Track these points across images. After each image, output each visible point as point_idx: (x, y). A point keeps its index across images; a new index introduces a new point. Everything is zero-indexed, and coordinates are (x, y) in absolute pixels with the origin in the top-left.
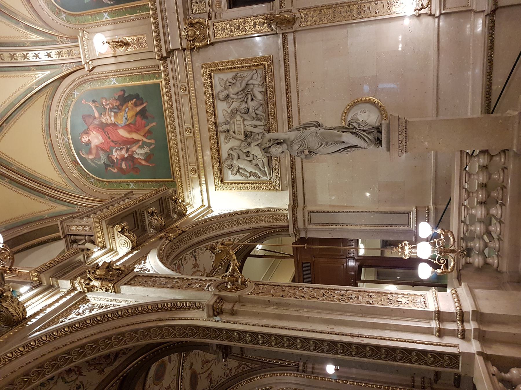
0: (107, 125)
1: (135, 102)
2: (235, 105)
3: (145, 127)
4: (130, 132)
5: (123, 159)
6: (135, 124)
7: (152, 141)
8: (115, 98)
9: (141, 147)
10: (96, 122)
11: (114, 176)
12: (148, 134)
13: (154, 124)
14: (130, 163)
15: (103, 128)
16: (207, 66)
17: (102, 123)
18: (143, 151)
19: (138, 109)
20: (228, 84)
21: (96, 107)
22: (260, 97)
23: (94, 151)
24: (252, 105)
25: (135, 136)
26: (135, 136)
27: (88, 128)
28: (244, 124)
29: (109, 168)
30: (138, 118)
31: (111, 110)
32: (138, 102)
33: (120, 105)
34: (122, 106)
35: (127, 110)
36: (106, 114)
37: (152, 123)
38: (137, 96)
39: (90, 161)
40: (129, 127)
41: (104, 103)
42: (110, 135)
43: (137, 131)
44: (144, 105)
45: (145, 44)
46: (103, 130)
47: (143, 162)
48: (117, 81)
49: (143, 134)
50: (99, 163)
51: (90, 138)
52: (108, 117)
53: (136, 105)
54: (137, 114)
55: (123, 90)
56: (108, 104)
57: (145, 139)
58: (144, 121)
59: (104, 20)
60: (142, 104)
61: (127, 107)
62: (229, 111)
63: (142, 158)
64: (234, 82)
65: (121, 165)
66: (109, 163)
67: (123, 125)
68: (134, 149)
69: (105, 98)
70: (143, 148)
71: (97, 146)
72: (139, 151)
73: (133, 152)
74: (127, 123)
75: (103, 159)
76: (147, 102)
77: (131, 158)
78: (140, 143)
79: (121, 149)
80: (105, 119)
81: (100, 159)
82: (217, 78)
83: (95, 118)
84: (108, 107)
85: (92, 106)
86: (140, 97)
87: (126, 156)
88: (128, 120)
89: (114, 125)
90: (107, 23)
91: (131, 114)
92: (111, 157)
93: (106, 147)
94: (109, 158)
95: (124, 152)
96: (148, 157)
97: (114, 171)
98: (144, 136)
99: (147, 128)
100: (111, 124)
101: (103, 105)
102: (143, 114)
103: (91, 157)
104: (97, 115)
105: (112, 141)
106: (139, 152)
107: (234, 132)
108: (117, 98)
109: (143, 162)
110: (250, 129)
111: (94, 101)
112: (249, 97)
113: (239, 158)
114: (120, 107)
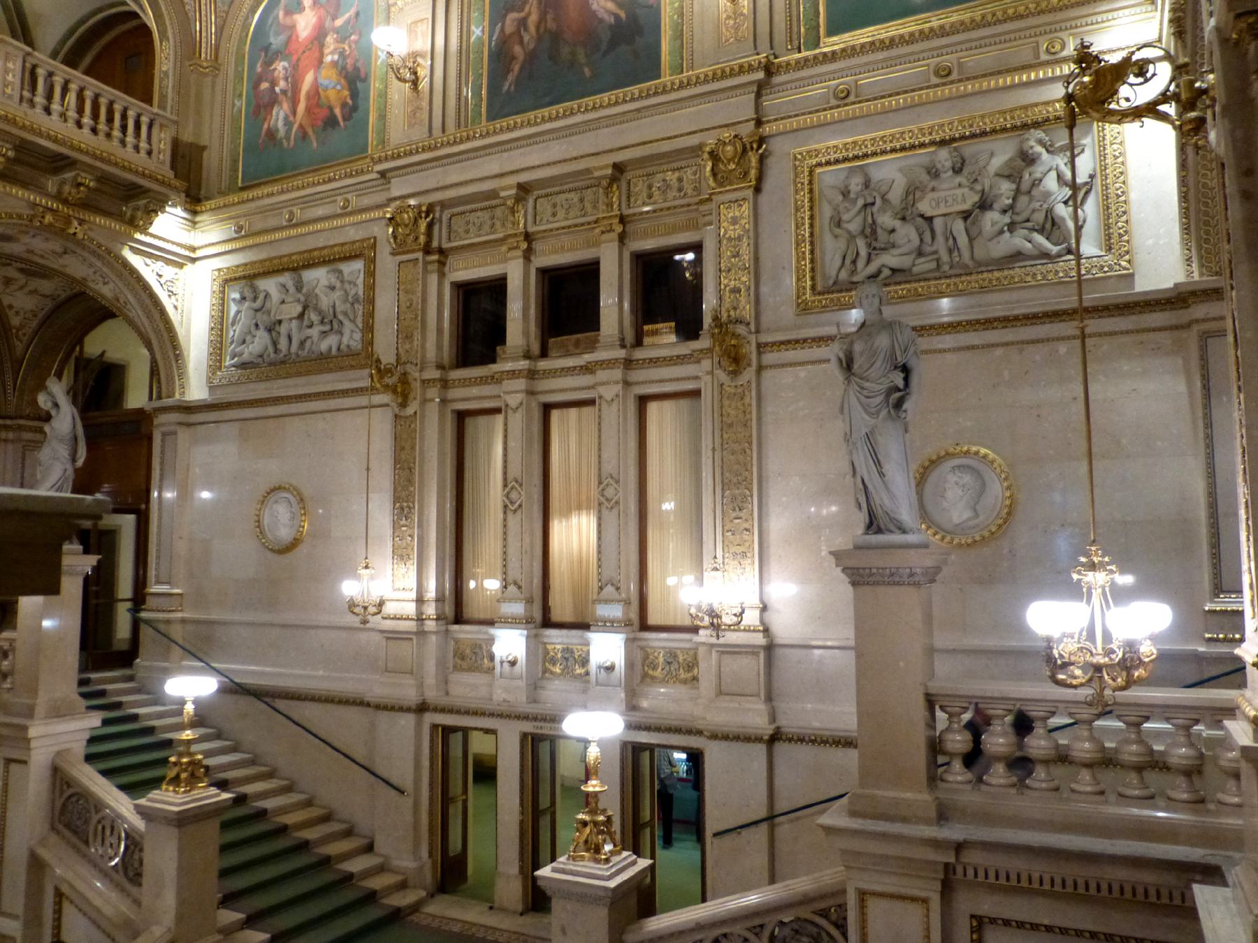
0: (322, 46)
1: (347, 103)
2: (325, 302)
3: (313, 126)
4: (308, 97)
5: (274, 83)
6: (318, 105)
7: (292, 143)
8: (357, 61)
9: (286, 118)
10: (328, 24)
11: (252, 67)
12: (304, 135)
13: (315, 144)
14: (266, 100)
15: (319, 36)
16: (374, 246)
17: (325, 35)
18: (280, 124)
19: (337, 111)
20: (347, 286)
21: (348, 22)
22: (324, 347)
23: (288, 21)
24: (314, 332)
25: (301, 107)
26: (301, 107)
27: (322, 6)
28: (291, 319)
29: (263, 54)
30: (323, 113)
31: (342, 54)
32: (347, 110)
33: (347, 72)
34: (346, 77)
35: (339, 87)
36: (338, 42)
37: (317, 139)
38: (355, 108)
39: (276, 12)
40: (315, 92)
41: (353, 37)
42: (307, 53)
43: (308, 110)
44: (342, 123)
45: (413, 121)
46: (316, 39)
47: (266, 126)
48: (382, 63)
49: (303, 123)
50: (271, 34)
51: (307, 10)
52: (332, 47)
53: (344, 105)
54: (331, 109)
55: (365, 80)
56: (350, 47)
57: (295, 127)
58: (320, 123)
59: (473, 28)
60: (344, 120)
61: (343, 88)
62: (317, 291)
63: (272, 122)
64: (350, 299)
65: (266, 81)
66: (270, 54)
67: (321, 81)
68: (286, 106)
69: (360, 38)
70: (285, 125)
71: (293, 27)
72: (282, 115)
73: (280, 104)
74: (320, 90)
75: (276, 41)
76: (346, 126)
77: (273, 101)
78: (291, 118)
79: (286, 79)
80: (330, 40)
81: (277, 34)
82: (358, 265)
83: (334, 19)
84: (347, 48)
85: (352, 12)
86: (354, 115)
87: (277, 89)
88: (325, 91)
89: (320, 62)
90: (464, 33)
91: (332, 94)
92: (276, 59)
93: (293, 46)
94: (278, 55)
95: (282, 84)
96: (271, 134)
97: (259, 65)
98: (301, 126)
99: (310, 131)
100: (322, 55)
101: (350, 36)
102: (331, 122)
103: (281, 14)
104: (339, 22)
105: (298, 60)
106: (279, 116)
107: (283, 302)
108: (359, 65)
109: (266, 126)
110: (283, 329)
111: (357, 14)
112: (327, 328)
113: (257, 311)
114: (344, 72)
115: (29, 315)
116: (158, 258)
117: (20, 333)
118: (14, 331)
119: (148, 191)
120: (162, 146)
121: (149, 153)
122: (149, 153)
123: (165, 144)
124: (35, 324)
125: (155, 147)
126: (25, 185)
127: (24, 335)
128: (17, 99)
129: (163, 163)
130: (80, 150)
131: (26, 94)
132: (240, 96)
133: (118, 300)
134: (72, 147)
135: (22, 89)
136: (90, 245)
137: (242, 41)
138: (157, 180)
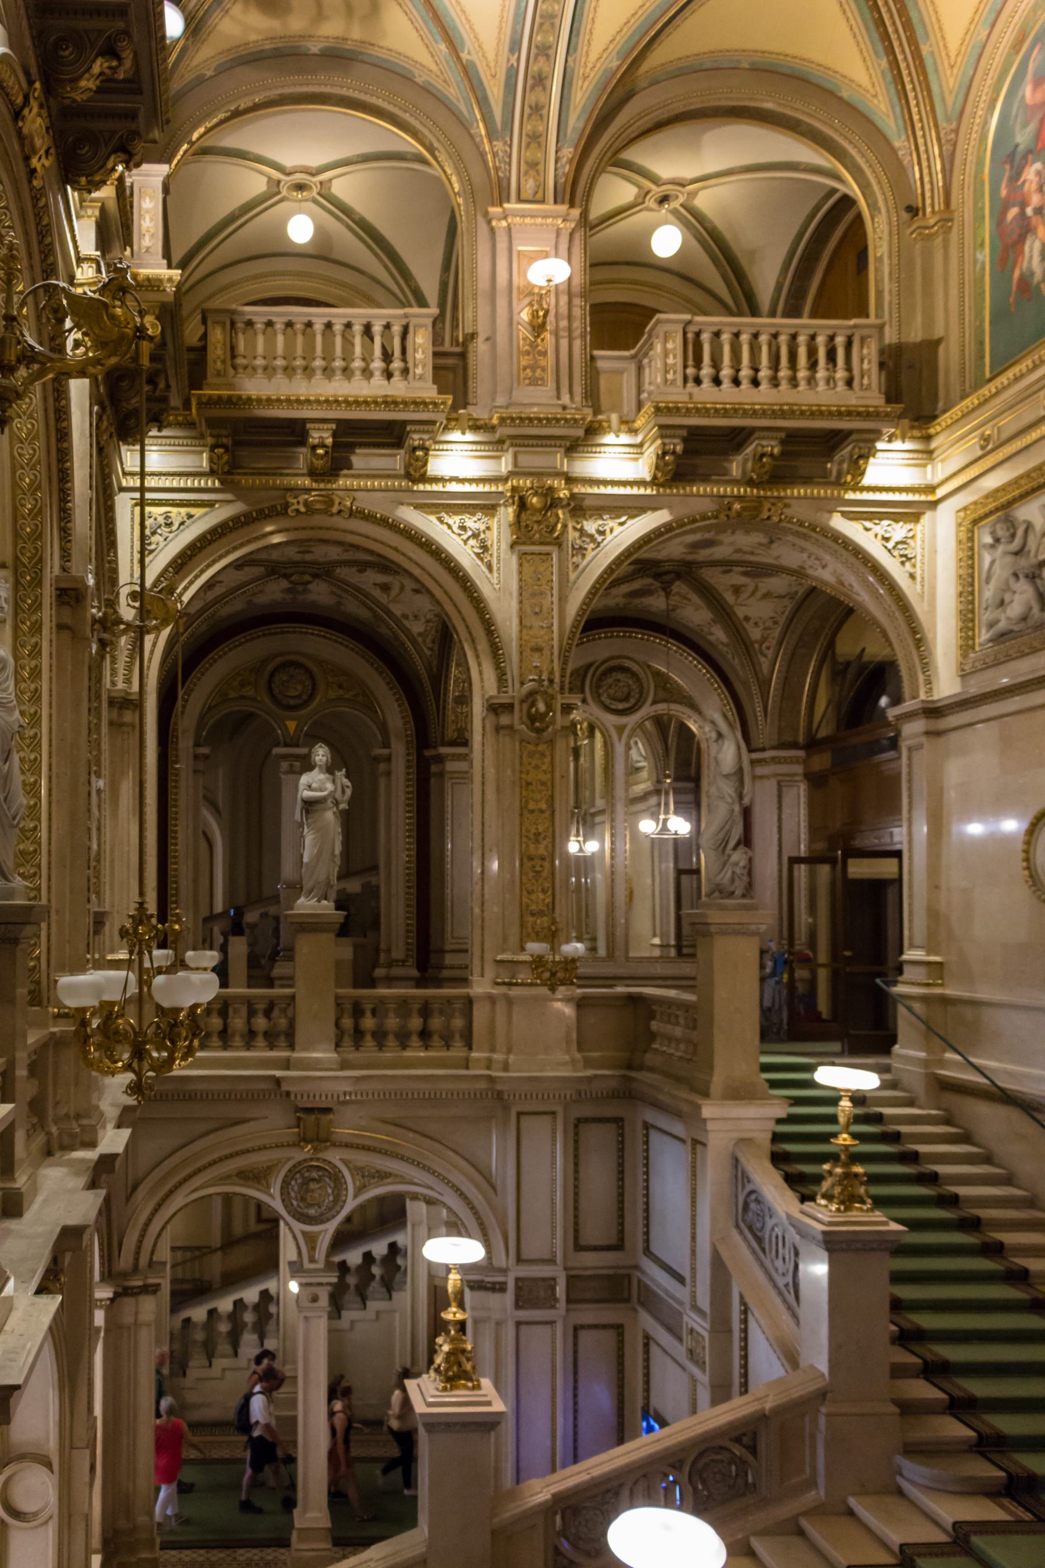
115: (769, 624)
116: (882, 517)
117: (764, 646)
118: (756, 646)
119: (850, 432)
120: (866, 366)
121: (849, 383)
122: (849, 383)
123: (870, 362)
124: (776, 633)
125: (856, 372)
126: (705, 479)
127: (768, 648)
128: (680, 381)
129: (869, 387)
130: (755, 414)
131: (690, 371)
132: (982, 245)
133: (843, 584)
134: (745, 413)
135: (685, 367)
136: (789, 526)
137: (980, 163)
138: (859, 414)
